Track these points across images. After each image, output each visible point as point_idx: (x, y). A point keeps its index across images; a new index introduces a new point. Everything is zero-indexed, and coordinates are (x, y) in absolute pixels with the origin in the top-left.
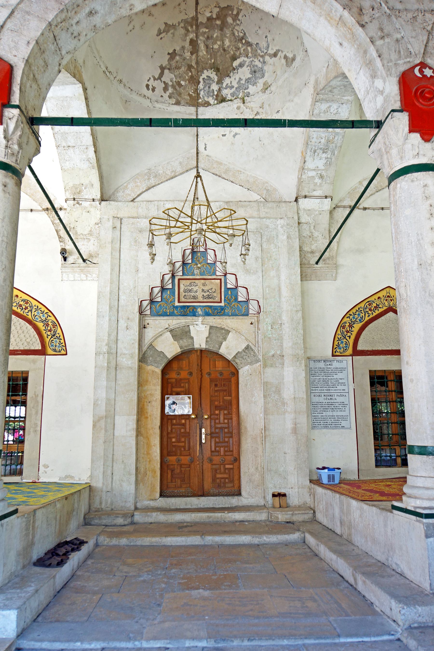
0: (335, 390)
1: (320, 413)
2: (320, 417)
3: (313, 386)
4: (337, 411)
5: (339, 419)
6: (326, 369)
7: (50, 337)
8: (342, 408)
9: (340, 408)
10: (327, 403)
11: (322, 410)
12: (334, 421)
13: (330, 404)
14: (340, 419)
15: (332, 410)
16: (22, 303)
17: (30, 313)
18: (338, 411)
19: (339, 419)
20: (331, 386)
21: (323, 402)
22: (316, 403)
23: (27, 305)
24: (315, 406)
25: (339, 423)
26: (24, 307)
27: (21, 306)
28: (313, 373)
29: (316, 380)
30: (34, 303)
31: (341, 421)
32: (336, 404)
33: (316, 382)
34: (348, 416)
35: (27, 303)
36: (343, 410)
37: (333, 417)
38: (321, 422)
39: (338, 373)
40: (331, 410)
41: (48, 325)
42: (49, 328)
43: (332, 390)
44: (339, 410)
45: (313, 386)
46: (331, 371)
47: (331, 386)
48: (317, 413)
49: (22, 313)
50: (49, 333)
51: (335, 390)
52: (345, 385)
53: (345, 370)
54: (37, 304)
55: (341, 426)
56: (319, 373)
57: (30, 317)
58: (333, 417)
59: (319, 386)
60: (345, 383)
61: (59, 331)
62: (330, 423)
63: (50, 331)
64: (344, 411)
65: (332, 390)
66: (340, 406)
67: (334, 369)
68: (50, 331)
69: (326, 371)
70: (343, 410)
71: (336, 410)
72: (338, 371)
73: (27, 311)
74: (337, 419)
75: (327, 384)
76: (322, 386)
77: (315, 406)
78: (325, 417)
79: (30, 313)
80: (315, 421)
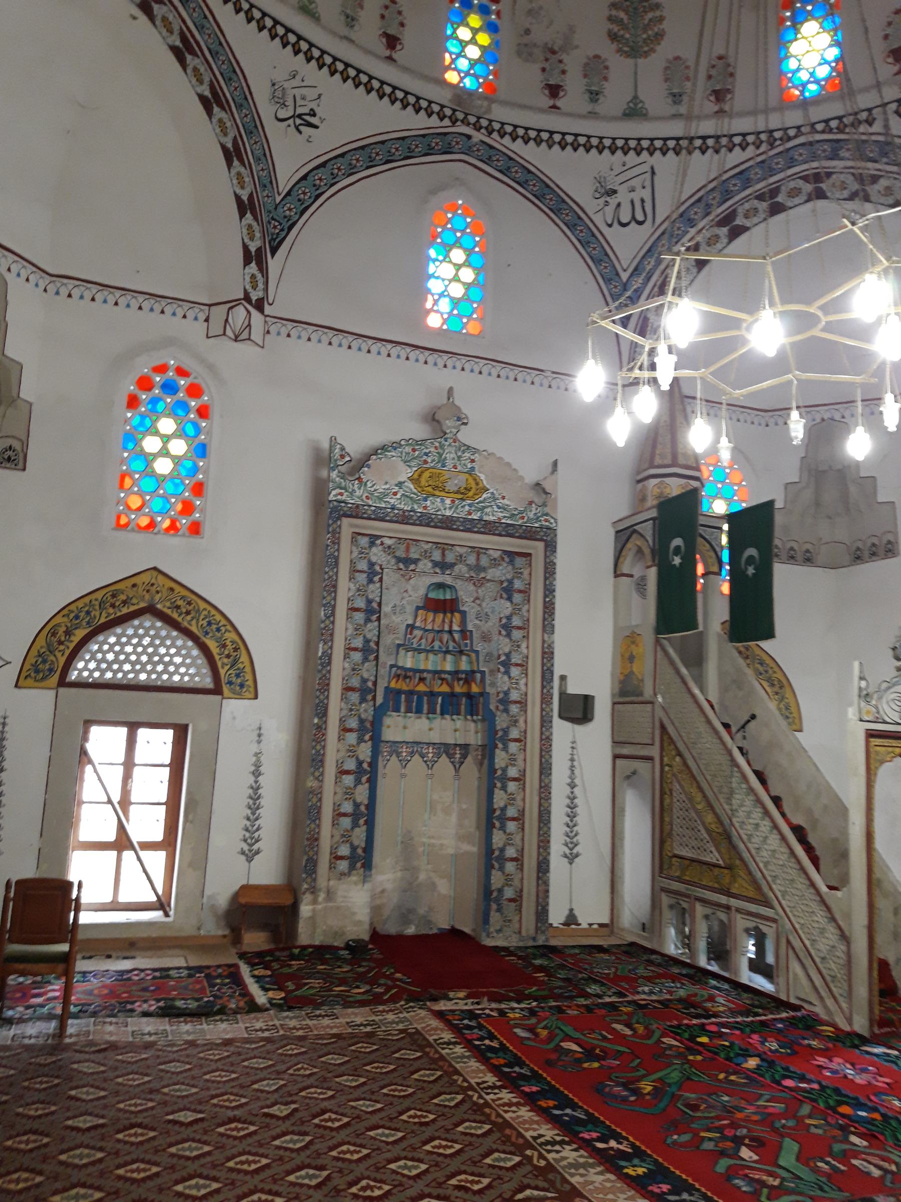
7: (227, 667)
16: (180, 603)
17: (194, 622)
23: (190, 608)
26: (184, 610)
27: (178, 607)
30: (202, 605)
35: (189, 603)
41: (224, 646)
42: (226, 652)
49: (180, 619)
50: (226, 660)
54: (209, 608)
57: (194, 629)
61: (244, 658)
63: (228, 656)
68: (228, 656)
73: (189, 618)
79: (194, 622)
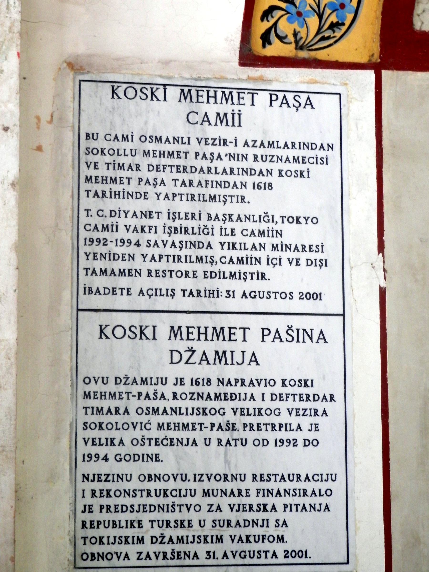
0: (254, 295)
1: (135, 458)
2: (134, 484)
3: (99, 265)
4: (257, 443)
5: (270, 501)
6: (194, 147)
8: (294, 421)
9: (285, 418)
10: (188, 388)
11: (155, 433)
12: (233, 517)
13: (213, 389)
14: (279, 502)
15: (224, 436)
18: (265, 442)
19: (270, 501)
20: (228, 268)
21: (163, 381)
22: (111, 387)
24: (106, 404)
25: (272, 531)
28: (102, 172)
29: (122, 221)
31: (281, 515)
32: (257, 391)
33: (122, 234)
34: (332, 477)
36: (300, 436)
37: (229, 486)
38: (146, 517)
39: (274, 179)
40: (215, 435)
43: (230, 294)
44: (271, 436)
45: (99, 265)
46: (226, 163)
47: (228, 268)
48: (118, 458)
51: (254, 295)
52: (323, 263)
53: (325, 161)
55: (279, 548)
56: (144, 174)
58: (229, 486)
59: (138, 263)
60: (320, 248)
62: (208, 531)
64: (307, 443)
65: (230, 294)
66: (283, 406)
67: (250, 152)
69: (191, 161)
70: (300, 436)
71: (250, 436)
72: (276, 167)
74: (254, 500)
75: (194, 253)
76: (162, 266)
77: (106, 404)
78: (171, 485)
80: (97, 516)
